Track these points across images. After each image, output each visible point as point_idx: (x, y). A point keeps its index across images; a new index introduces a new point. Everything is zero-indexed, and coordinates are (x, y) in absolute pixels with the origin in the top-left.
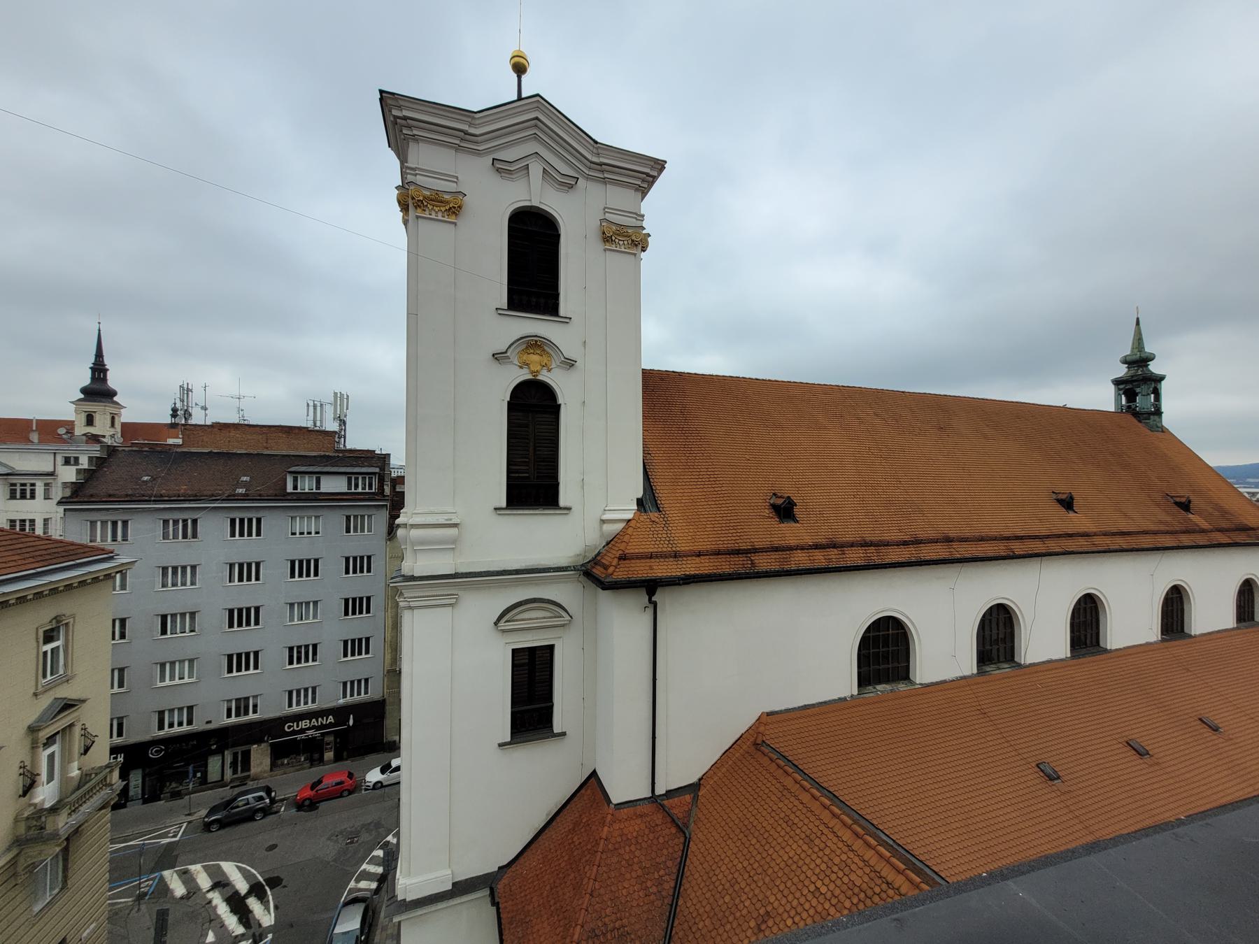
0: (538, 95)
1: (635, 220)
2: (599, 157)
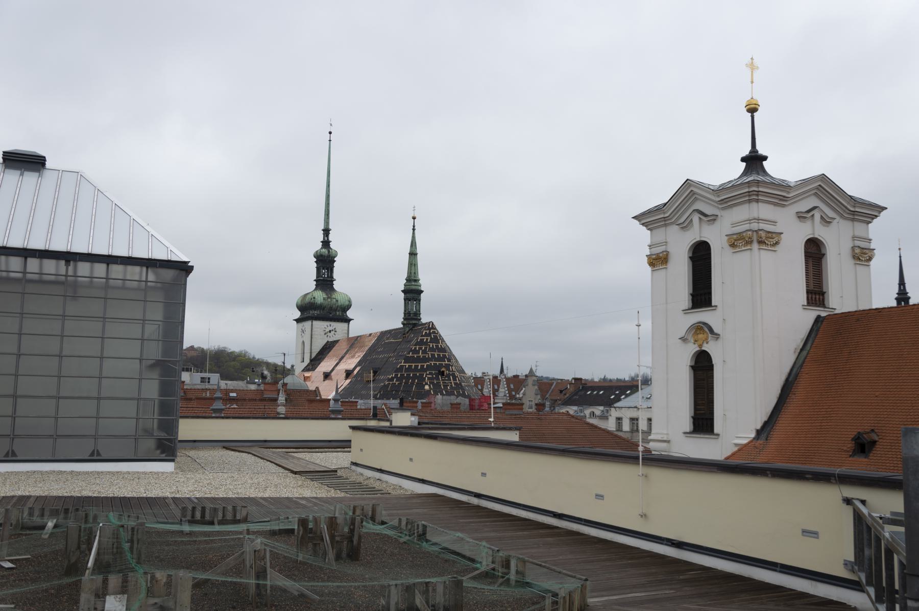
0: (688, 180)
1: (748, 225)
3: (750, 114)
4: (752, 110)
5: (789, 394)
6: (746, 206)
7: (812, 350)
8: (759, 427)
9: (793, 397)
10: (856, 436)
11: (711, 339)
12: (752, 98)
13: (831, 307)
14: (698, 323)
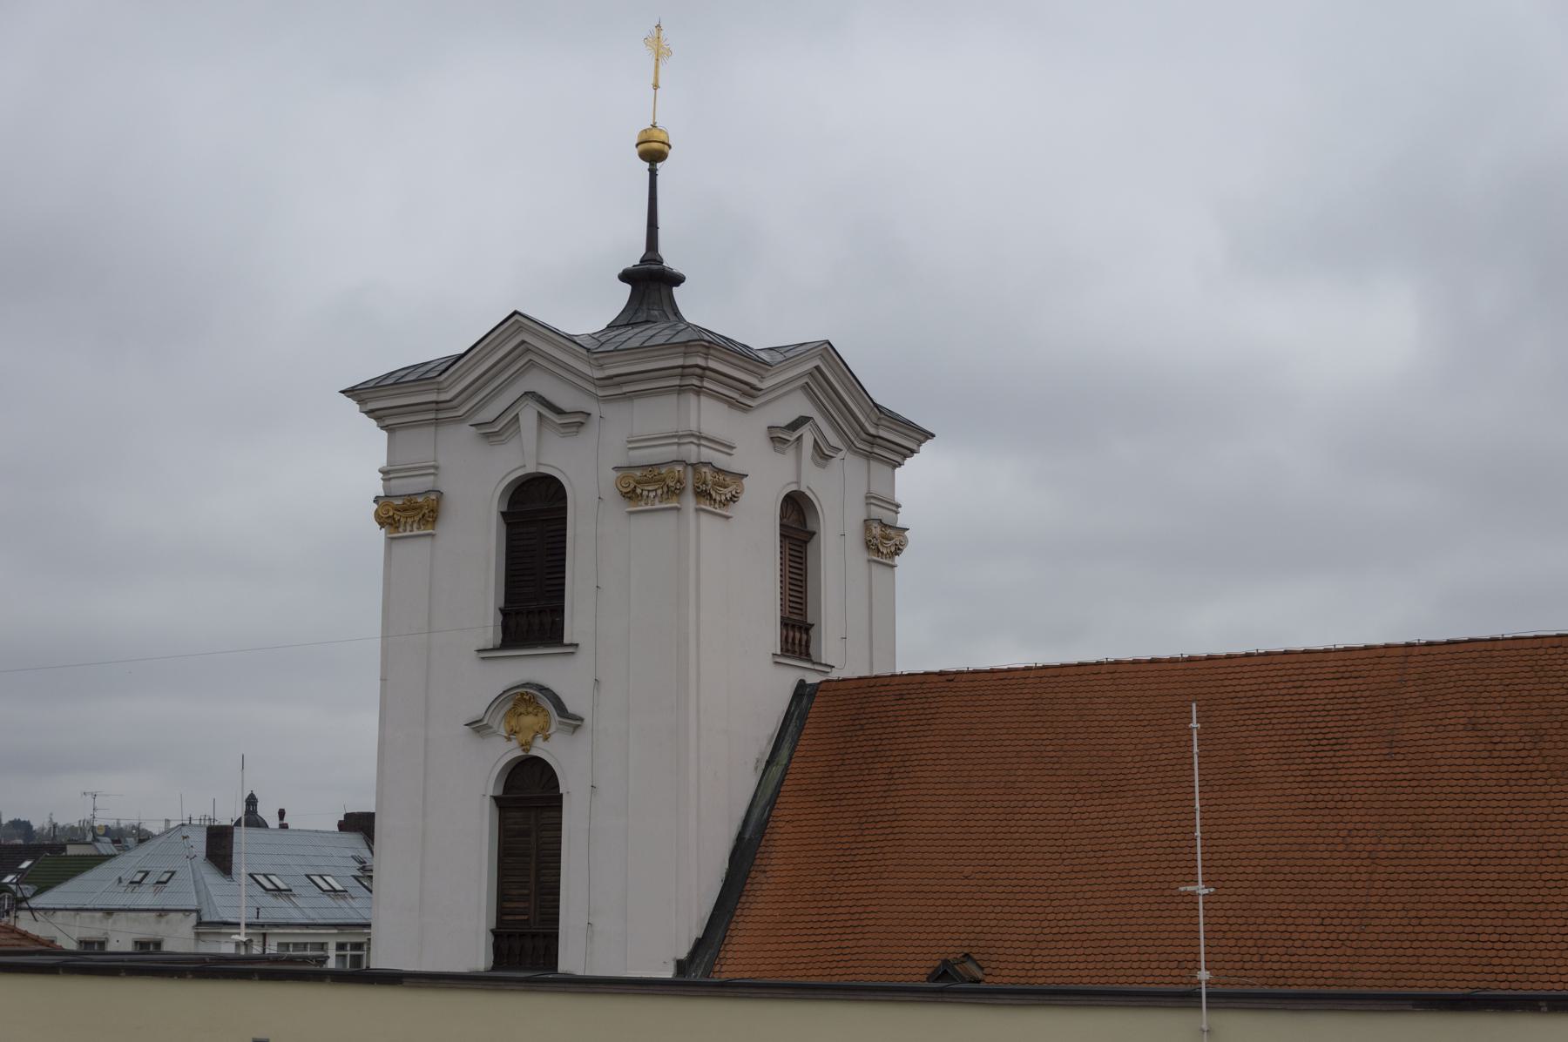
0: (515, 313)
1: (675, 447)
2: (603, 369)
3: (647, 165)
4: (653, 155)
5: (750, 872)
6: (670, 401)
7: (795, 765)
8: (683, 954)
9: (761, 877)
10: (937, 969)
11: (558, 729)
12: (654, 126)
13: (823, 662)
14: (524, 686)
